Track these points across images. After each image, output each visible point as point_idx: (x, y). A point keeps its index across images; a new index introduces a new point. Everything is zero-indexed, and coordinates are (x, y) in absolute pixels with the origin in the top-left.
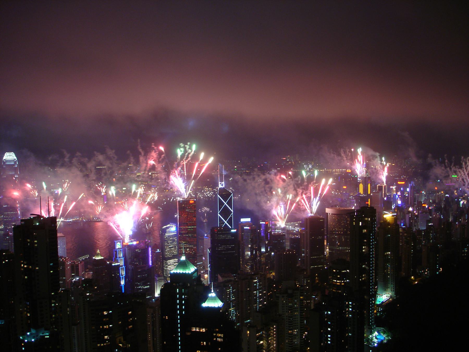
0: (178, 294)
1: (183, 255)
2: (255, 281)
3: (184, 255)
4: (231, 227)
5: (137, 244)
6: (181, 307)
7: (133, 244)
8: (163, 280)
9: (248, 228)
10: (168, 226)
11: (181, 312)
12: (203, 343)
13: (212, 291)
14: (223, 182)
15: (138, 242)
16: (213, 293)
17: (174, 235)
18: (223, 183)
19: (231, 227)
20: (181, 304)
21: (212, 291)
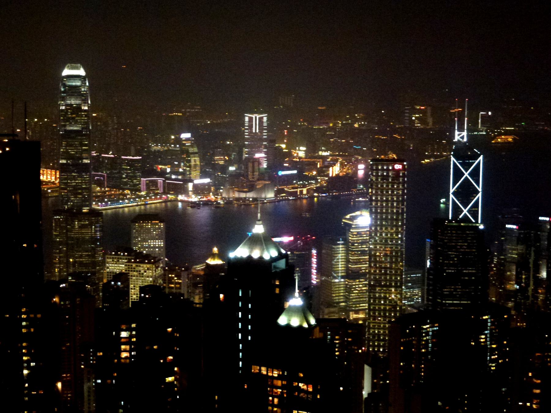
0: (240, 299)
1: (258, 222)
2: (484, 317)
3: (261, 222)
4: (474, 221)
5: (291, 241)
6: (245, 326)
7: (282, 240)
8: (337, 314)
9: (514, 227)
10: (358, 213)
11: (245, 337)
12: (273, 400)
13: (297, 294)
14: (464, 131)
15: (292, 238)
16: (297, 298)
17: (367, 231)
18: (465, 133)
19: (474, 221)
20: (244, 320)
21: (297, 294)
